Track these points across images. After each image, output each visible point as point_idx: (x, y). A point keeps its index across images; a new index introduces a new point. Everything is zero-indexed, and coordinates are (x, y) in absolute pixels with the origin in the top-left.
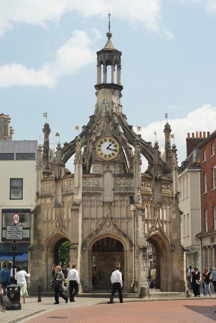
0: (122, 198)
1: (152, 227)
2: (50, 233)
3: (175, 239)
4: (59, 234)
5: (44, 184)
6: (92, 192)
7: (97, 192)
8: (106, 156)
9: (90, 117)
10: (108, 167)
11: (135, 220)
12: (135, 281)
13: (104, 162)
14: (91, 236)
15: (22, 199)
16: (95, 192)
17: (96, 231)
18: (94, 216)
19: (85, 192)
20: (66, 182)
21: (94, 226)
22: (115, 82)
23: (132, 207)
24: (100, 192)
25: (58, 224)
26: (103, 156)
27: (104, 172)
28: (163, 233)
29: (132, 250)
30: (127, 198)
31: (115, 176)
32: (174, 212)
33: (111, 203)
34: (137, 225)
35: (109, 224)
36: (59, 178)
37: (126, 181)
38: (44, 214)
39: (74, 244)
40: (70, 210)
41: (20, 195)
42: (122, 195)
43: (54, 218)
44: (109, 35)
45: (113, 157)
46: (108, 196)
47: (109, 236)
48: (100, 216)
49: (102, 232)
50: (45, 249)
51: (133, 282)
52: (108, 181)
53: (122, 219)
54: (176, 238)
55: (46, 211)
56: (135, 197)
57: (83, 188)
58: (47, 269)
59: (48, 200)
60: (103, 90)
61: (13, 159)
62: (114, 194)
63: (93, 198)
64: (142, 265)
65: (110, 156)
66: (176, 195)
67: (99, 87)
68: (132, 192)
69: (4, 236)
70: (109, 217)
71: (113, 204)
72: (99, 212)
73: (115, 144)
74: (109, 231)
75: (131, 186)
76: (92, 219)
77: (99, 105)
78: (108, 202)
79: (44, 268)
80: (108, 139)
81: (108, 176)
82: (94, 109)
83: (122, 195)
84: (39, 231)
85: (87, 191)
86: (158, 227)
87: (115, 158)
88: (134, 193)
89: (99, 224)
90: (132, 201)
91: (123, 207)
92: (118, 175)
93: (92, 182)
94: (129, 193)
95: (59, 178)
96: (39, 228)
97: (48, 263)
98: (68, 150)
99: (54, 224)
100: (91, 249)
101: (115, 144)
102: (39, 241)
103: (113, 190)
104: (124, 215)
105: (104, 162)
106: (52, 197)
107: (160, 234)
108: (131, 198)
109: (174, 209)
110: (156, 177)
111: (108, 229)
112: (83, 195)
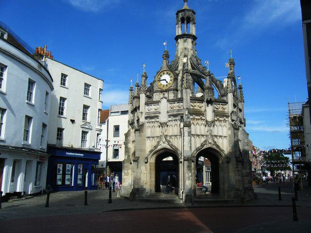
0: (174, 118)
1: (205, 141)
6: (152, 115)
7: (156, 115)
10: (164, 94)
16: (154, 115)
24: (158, 115)
28: (218, 146)
30: (179, 118)
31: (169, 101)
33: (166, 123)
42: (175, 116)
45: (169, 86)
46: (163, 118)
49: (159, 147)
52: (164, 107)
56: (185, 117)
63: (153, 120)
66: (231, 114)
68: (183, 112)
72: (158, 131)
74: (164, 145)
78: (165, 123)
80: (165, 72)
81: (164, 101)
83: (175, 116)
84: (129, 149)
89: (158, 140)
91: (176, 126)
93: (153, 108)
94: (179, 114)
96: (129, 147)
105: (162, 91)
107: (214, 147)
108: (182, 117)
111: (164, 145)
112: (146, 118)
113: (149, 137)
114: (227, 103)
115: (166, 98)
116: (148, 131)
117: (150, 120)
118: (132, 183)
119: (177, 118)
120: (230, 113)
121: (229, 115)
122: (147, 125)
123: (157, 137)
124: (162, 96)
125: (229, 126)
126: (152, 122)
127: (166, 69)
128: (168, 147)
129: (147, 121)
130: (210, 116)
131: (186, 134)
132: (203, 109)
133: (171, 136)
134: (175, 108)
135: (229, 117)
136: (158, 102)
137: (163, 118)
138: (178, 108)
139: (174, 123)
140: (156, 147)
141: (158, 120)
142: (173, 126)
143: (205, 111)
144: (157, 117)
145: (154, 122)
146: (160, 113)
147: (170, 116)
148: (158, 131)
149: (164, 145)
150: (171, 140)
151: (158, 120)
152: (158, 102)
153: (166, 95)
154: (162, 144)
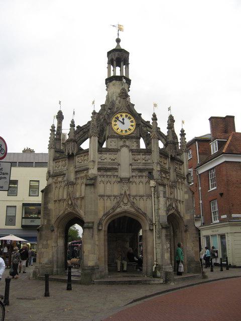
0: (140, 174)
1: (170, 205)
2: (62, 212)
3: (188, 220)
4: (70, 213)
5: (56, 162)
6: (108, 166)
7: (114, 167)
8: (122, 131)
9: (101, 106)
10: (125, 142)
11: (156, 196)
12: (157, 264)
13: (121, 137)
14: (106, 214)
15: (30, 181)
16: (111, 166)
17: (113, 209)
18: (108, 193)
19: (100, 166)
20: (77, 159)
21: (109, 204)
22: (124, 75)
23: (153, 183)
24: (117, 167)
25: (70, 202)
26: (119, 131)
27: (122, 147)
28: (178, 213)
29: (153, 229)
31: (132, 151)
32: (186, 193)
34: (159, 201)
35: (127, 201)
36: (73, 153)
37: (144, 157)
38: (54, 194)
39: (88, 223)
40: (83, 186)
41: (37, 193)
42: (140, 170)
43: (65, 197)
44: (118, 41)
45: (129, 132)
46: (125, 172)
47: (128, 215)
48: (116, 193)
49: (118, 210)
50: (56, 229)
51: (155, 266)
52: (125, 156)
53: (141, 196)
54: (189, 218)
55: (57, 189)
57: (98, 162)
58: (57, 251)
59: (60, 179)
60: (114, 82)
61: (32, 166)
62: (132, 169)
63: (109, 173)
64: (165, 247)
65: (126, 131)
66: (187, 176)
67: (109, 80)
68: (151, 167)
69: (23, 224)
70: (128, 193)
71: (131, 180)
72: (115, 189)
73: (131, 120)
75: (149, 161)
76: (109, 196)
77: (110, 95)
78: (126, 178)
79: (55, 250)
81: (125, 151)
82: (105, 99)
85: (102, 166)
86: (174, 206)
87: (131, 134)
88: (153, 169)
90: (150, 175)
91: (141, 184)
92: (136, 150)
93: (108, 157)
94: (147, 169)
95: (73, 153)
97: (58, 244)
98: (81, 133)
99: (65, 203)
100: (106, 229)
101: (131, 120)
102: (49, 221)
103: (131, 165)
104: (142, 192)
106: (64, 174)
108: (150, 173)
109: (186, 190)
110: (171, 156)
112: (99, 169)
113: (102, 196)
114: (183, 163)
115: (127, 146)
116: (101, 188)
117: (105, 174)
118: (55, 258)
119: (144, 174)
120: (186, 174)
121: (186, 177)
122: (99, 179)
123: (115, 197)
124: (121, 143)
125: (186, 190)
126: (107, 176)
127: (125, 111)
128: (132, 210)
129: (99, 173)
130: (172, 176)
131: (161, 195)
132: (167, 166)
133: (135, 197)
134: (139, 161)
135: (186, 180)
136: (116, 151)
137: (125, 172)
138: (144, 161)
139: (137, 180)
140: (114, 209)
141: (116, 174)
142: (138, 182)
143: (169, 168)
144: (116, 169)
145: (110, 176)
146: (119, 165)
147: (133, 170)
148: (115, 189)
149: (126, 208)
150: (135, 201)
151: (116, 174)
152: (116, 151)
153: (128, 143)
154: (123, 206)
